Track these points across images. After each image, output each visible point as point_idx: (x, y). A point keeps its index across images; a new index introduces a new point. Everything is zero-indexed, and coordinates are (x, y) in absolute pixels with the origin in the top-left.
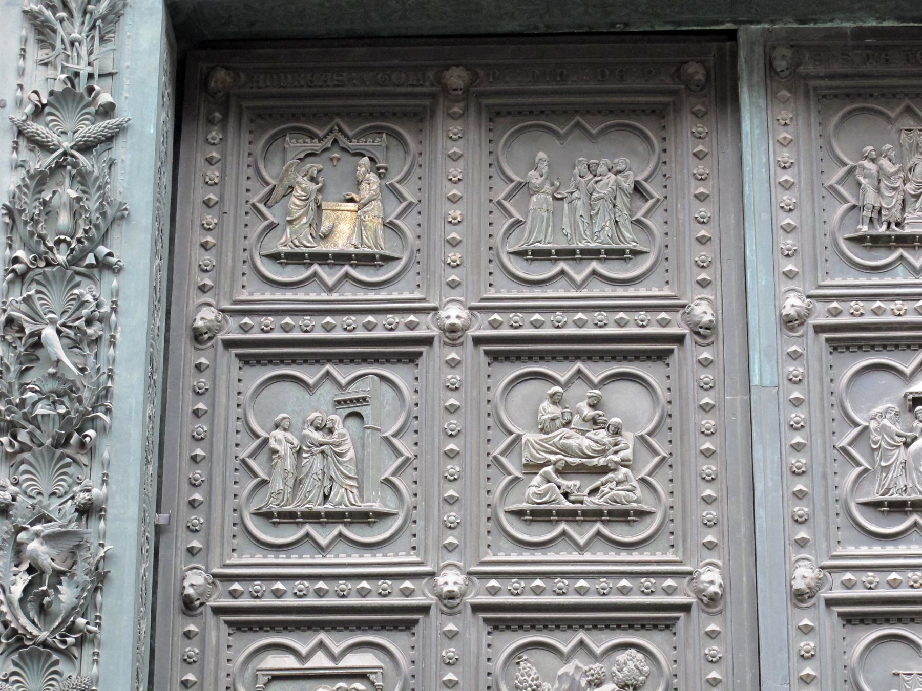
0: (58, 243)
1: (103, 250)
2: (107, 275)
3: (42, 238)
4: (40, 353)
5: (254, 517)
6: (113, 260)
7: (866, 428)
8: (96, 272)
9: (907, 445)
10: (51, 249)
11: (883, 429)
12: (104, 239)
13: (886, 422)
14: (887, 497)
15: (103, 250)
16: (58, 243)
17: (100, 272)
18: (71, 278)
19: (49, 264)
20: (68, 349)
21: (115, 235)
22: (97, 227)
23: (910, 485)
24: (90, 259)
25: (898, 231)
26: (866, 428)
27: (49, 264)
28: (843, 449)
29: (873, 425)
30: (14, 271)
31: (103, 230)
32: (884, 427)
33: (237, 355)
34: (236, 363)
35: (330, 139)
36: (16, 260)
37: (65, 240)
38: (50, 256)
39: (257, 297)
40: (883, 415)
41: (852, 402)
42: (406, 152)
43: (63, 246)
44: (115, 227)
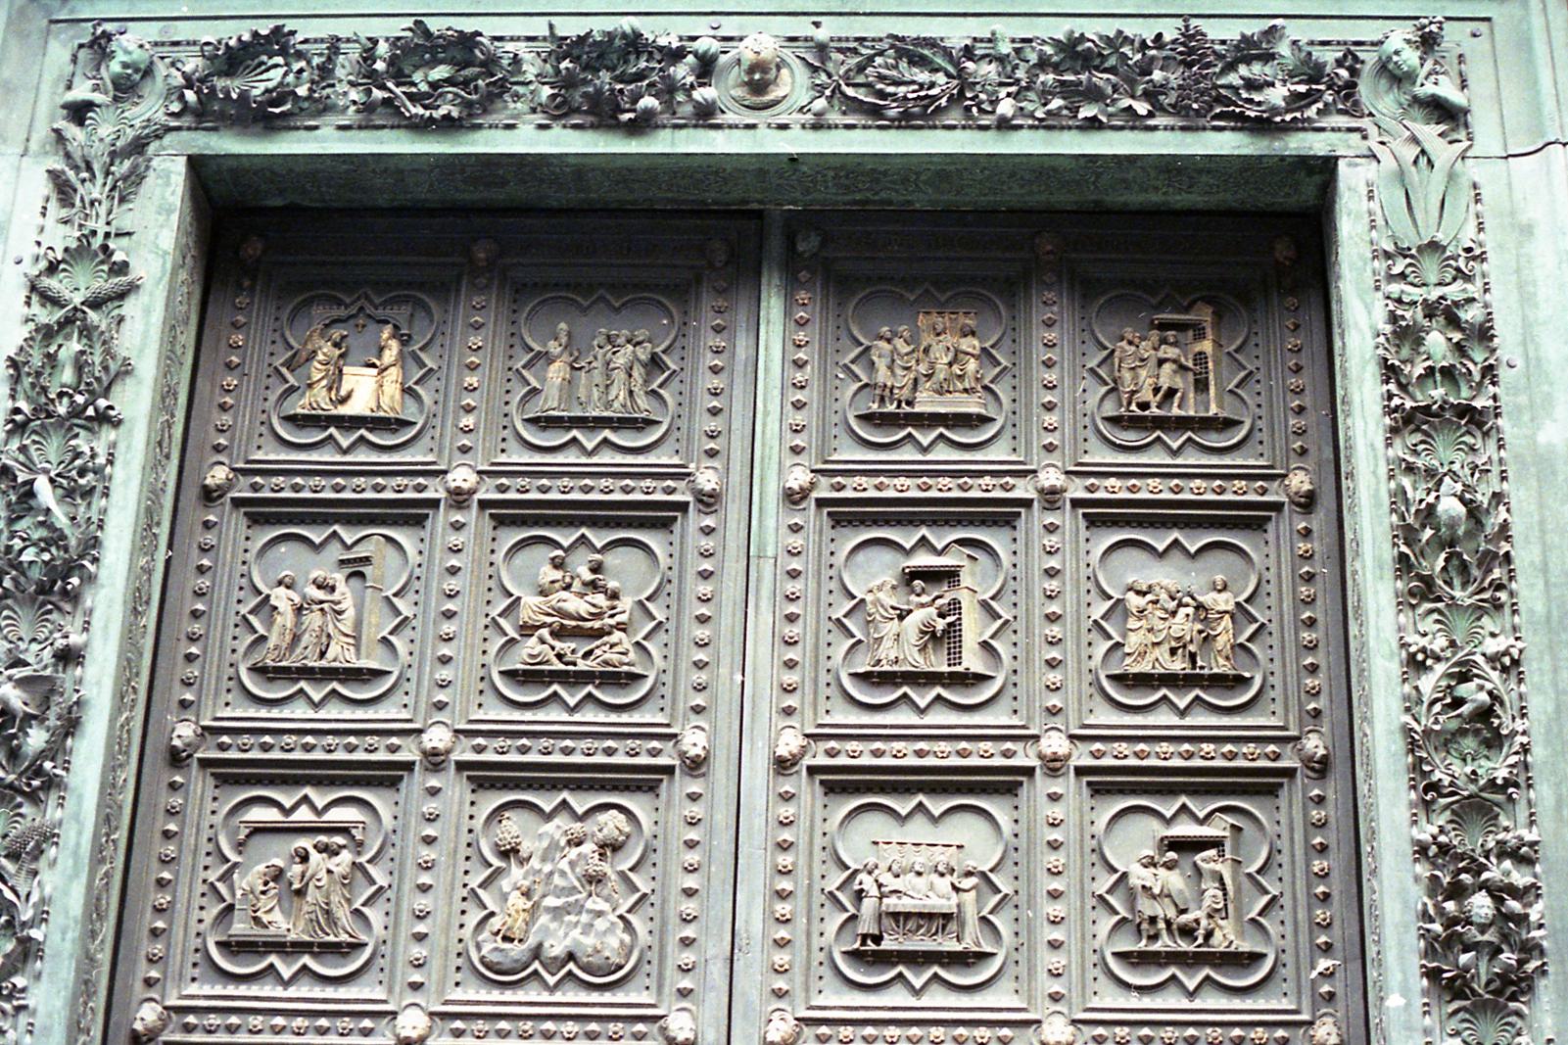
0: (61, 395)
1: (102, 403)
2: (105, 428)
3: (44, 390)
4: (33, 503)
5: (253, 674)
6: (112, 413)
7: (863, 601)
8: (96, 426)
9: (901, 618)
10: (52, 401)
11: (877, 602)
12: (106, 392)
13: (881, 595)
14: (877, 669)
15: (102, 403)
16: (61, 395)
17: (100, 426)
18: (70, 429)
19: (49, 415)
20: (60, 501)
21: (116, 389)
22: (98, 379)
23: (901, 657)
24: (90, 412)
25: (908, 409)
26: (863, 601)
27: (49, 415)
28: (838, 620)
29: (869, 598)
30: (13, 421)
31: (106, 384)
32: (878, 600)
33: (245, 514)
34: (244, 522)
35: (359, 304)
36: (17, 411)
37: (67, 393)
38: (51, 408)
39: (272, 457)
40: (880, 588)
41: (852, 576)
42: (432, 321)
43: (65, 400)
44: (119, 382)
